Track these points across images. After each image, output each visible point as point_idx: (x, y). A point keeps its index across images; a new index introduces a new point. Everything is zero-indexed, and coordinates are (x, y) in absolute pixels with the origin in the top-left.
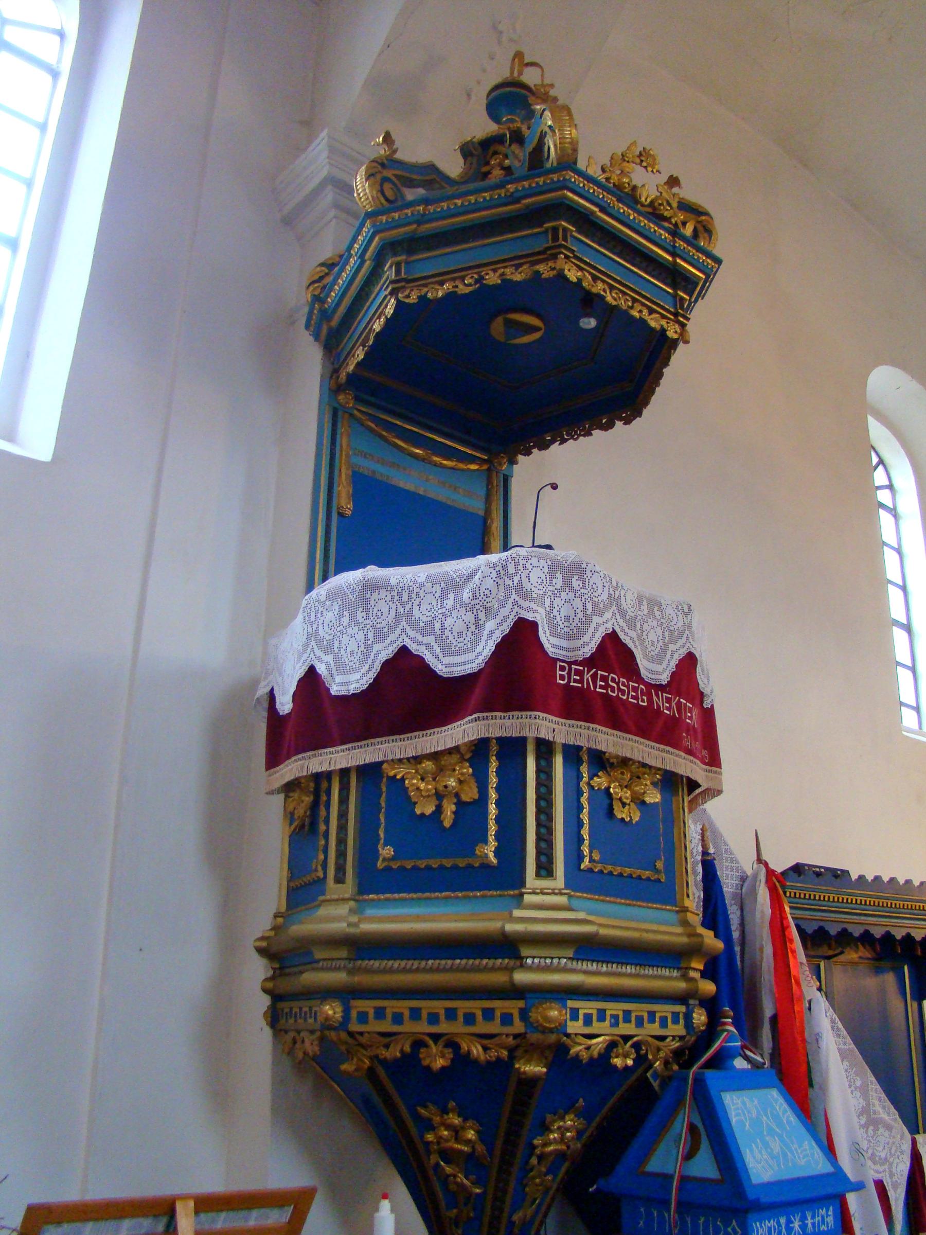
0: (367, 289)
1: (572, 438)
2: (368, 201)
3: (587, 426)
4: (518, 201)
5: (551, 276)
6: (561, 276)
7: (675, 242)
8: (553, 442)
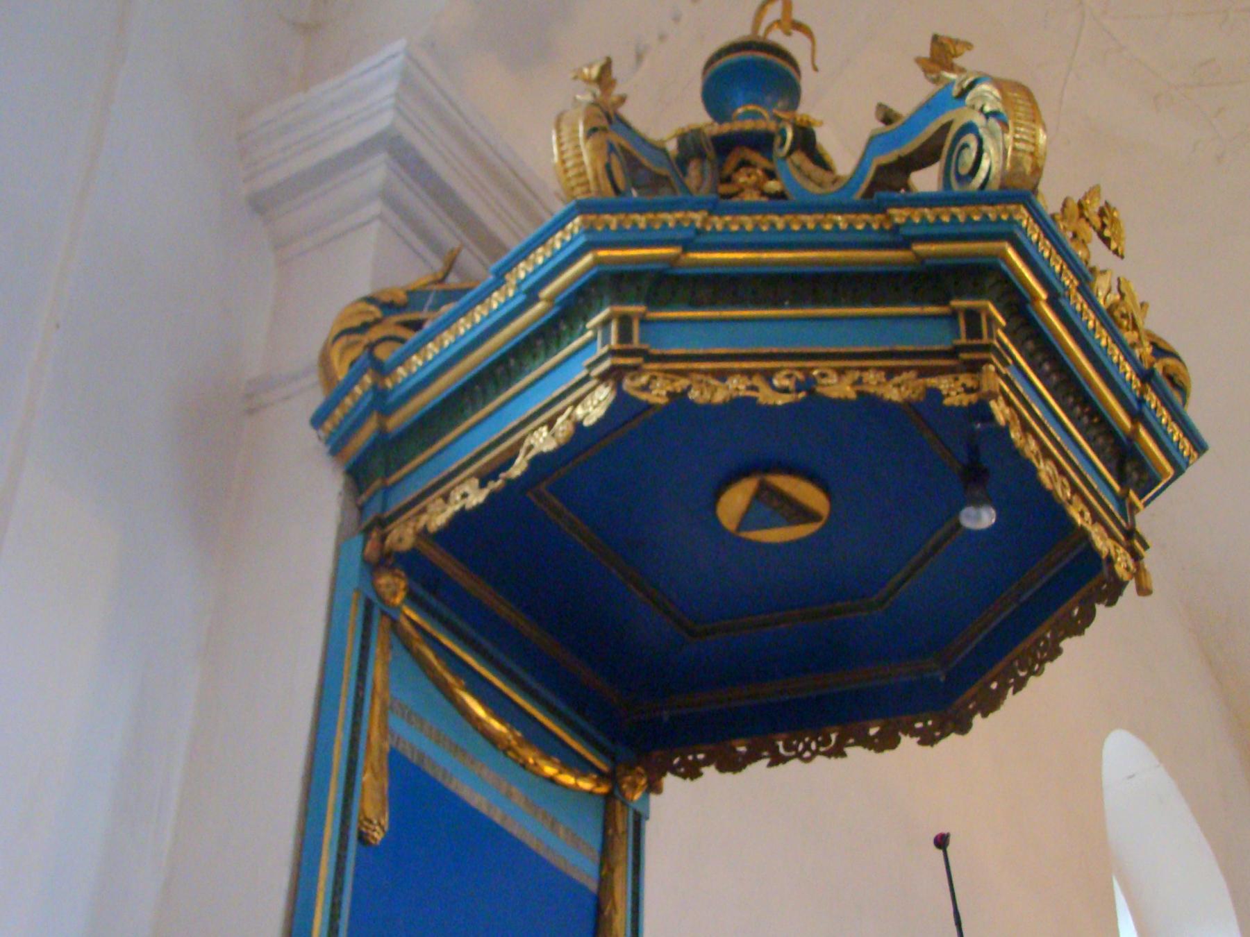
0: (512, 362)
1: (799, 756)
2: (582, 180)
3: (833, 737)
4: (905, 244)
5: (965, 403)
6: (981, 411)
7: (1143, 392)
8: (752, 757)
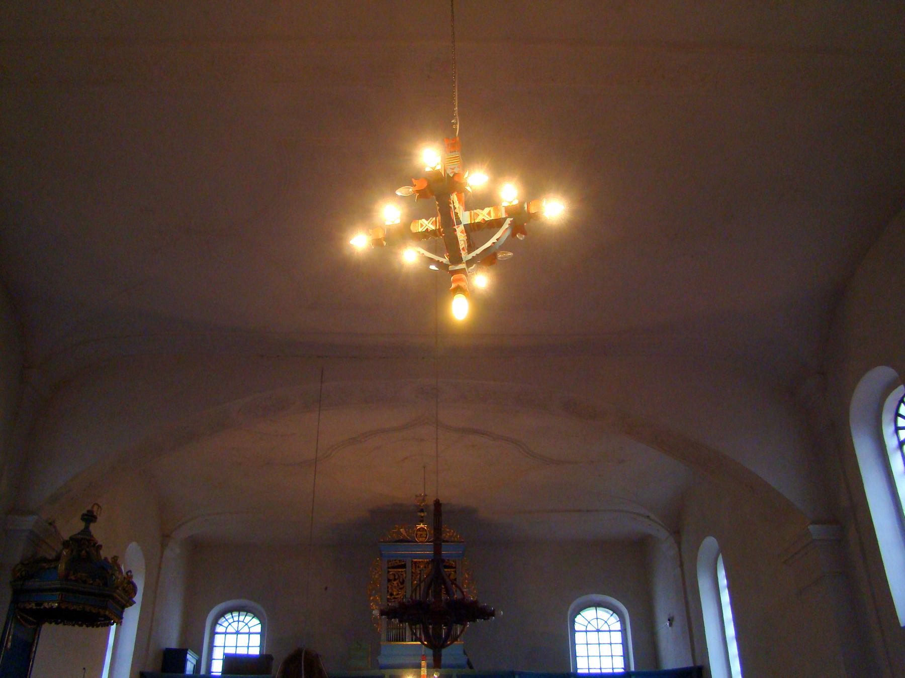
8: (60, 623)
